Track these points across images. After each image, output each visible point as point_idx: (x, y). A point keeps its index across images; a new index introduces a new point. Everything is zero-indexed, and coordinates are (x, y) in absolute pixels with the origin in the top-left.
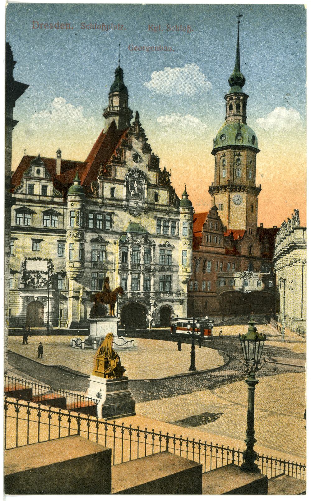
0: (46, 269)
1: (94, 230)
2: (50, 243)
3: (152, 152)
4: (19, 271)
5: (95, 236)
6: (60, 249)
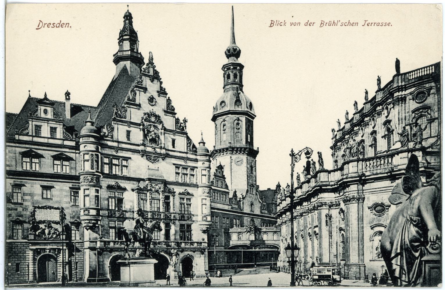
0: (57, 218)
2: (61, 191)
4: (27, 221)
5: (112, 182)
6: (73, 197)
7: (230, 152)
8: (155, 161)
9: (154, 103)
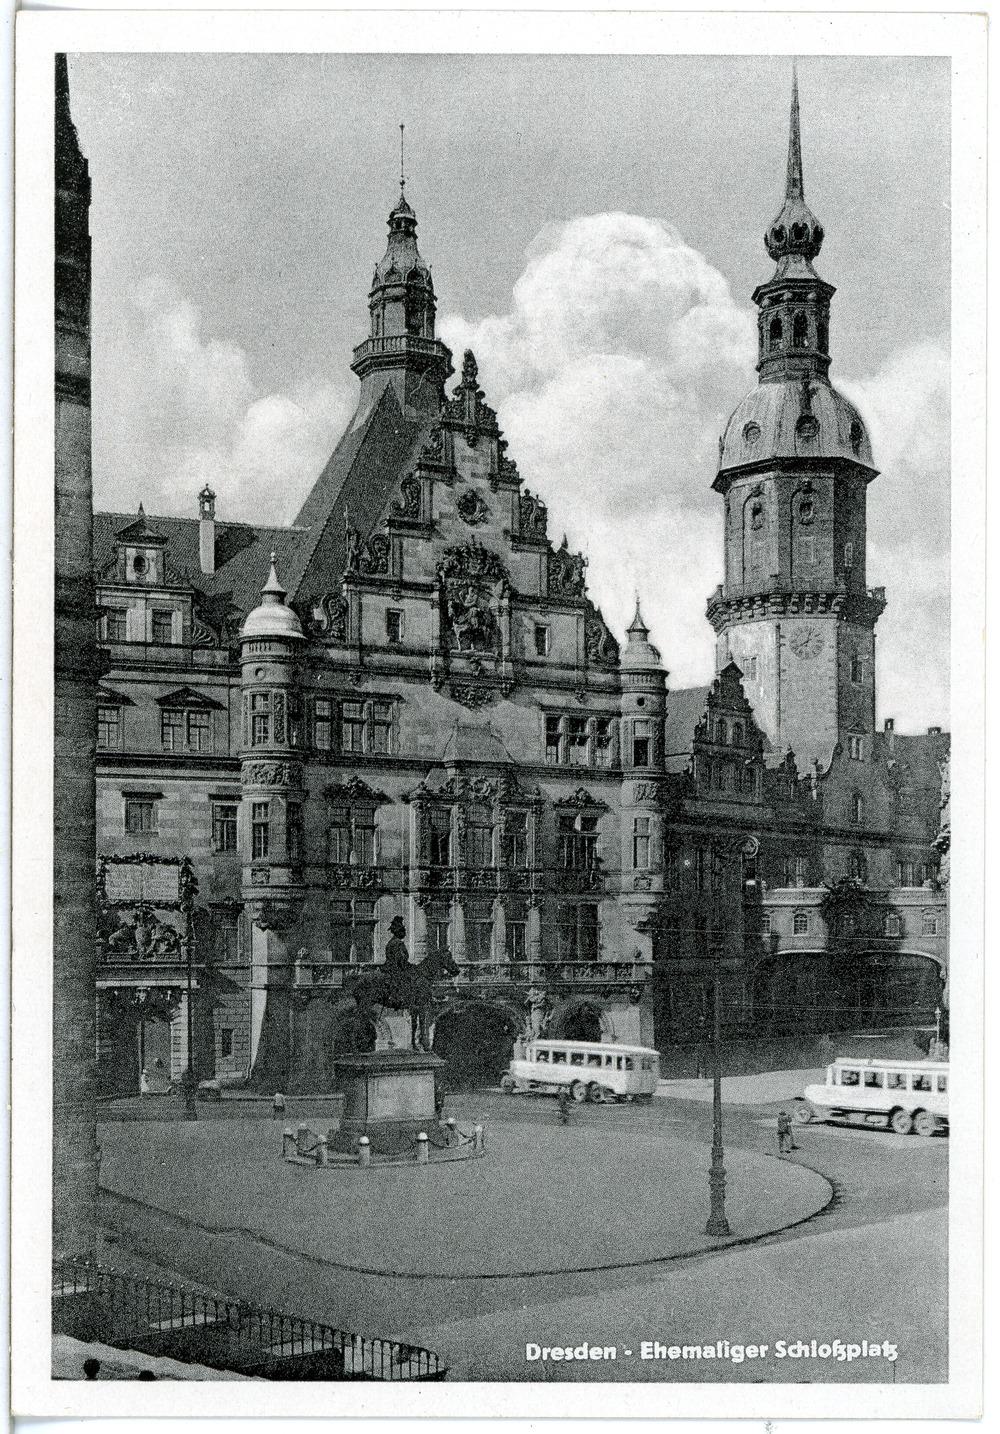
0: (173, 894)
1: (334, 759)
3: (522, 488)
7: (774, 609)
8: (476, 702)
9: (477, 515)
